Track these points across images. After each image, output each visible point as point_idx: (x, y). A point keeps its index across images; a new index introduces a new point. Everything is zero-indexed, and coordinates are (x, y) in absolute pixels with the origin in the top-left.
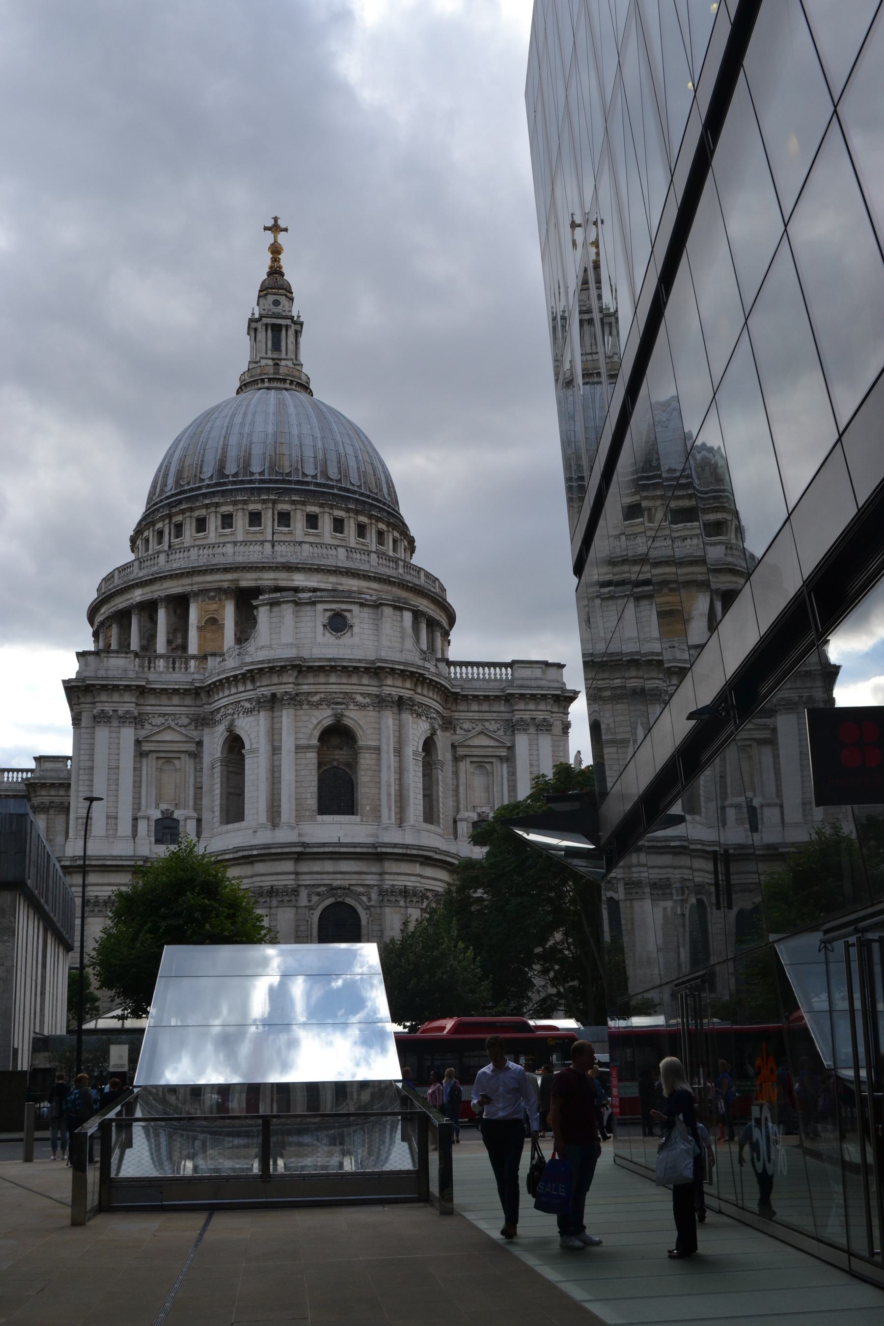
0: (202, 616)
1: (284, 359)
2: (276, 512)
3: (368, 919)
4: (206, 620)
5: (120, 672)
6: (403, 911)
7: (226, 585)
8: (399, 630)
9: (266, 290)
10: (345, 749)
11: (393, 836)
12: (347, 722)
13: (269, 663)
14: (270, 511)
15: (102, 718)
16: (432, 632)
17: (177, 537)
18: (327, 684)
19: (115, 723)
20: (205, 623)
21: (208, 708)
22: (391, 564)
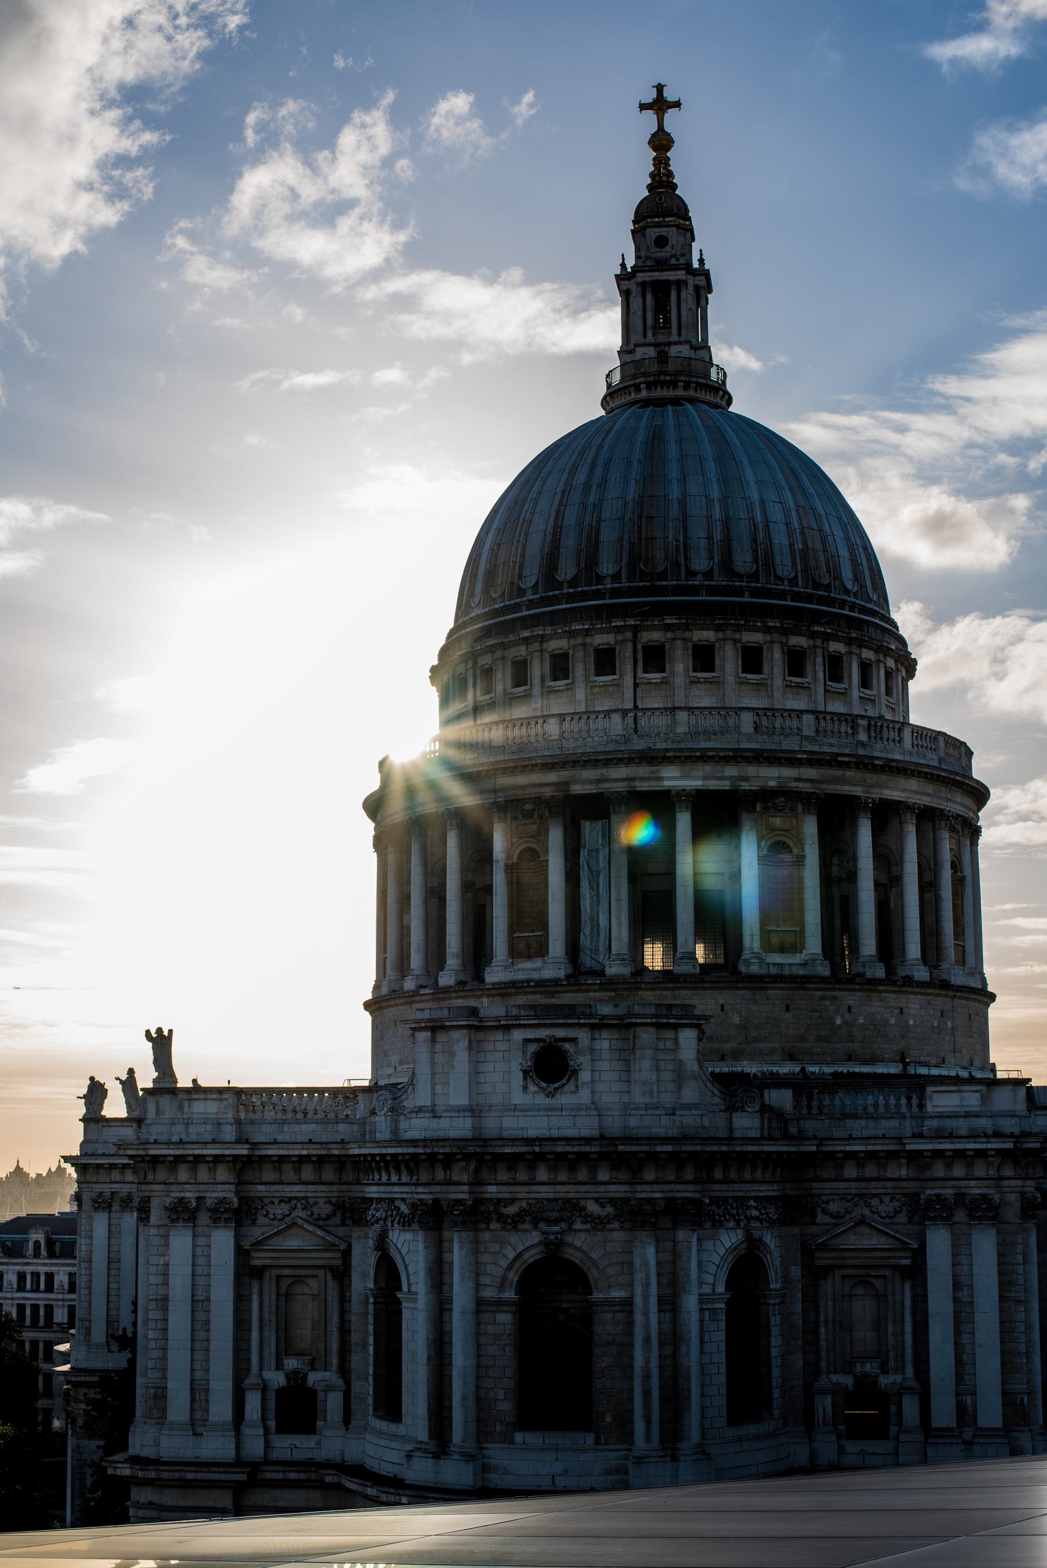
0: (512, 845)
1: (676, 343)
2: (639, 647)
4: (520, 853)
5: (209, 1127)
7: (548, 792)
9: (645, 218)
12: (569, 1254)
13: (425, 1147)
14: (630, 645)
16: (934, 830)
19: (203, 1218)
20: (519, 858)
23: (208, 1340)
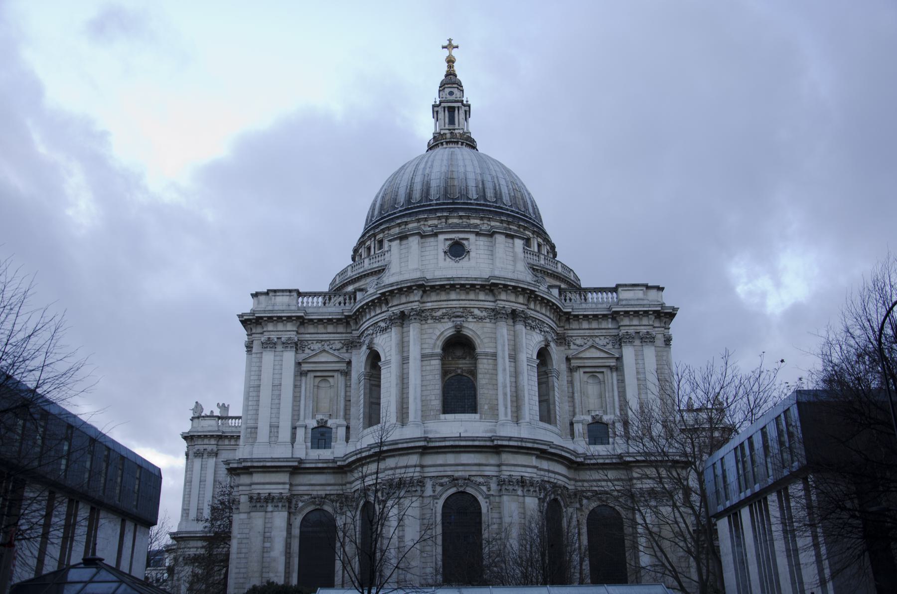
3: (488, 507)
6: (521, 499)
8: (511, 254)
10: (468, 358)
11: (508, 430)
12: (466, 332)
13: (397, 285)
15: (269, 344)
17: (380, 249)
18: (448, 301)
19: (279, 348)
21: (356, 333)
22: (535, 257)
23: (280, 404)
